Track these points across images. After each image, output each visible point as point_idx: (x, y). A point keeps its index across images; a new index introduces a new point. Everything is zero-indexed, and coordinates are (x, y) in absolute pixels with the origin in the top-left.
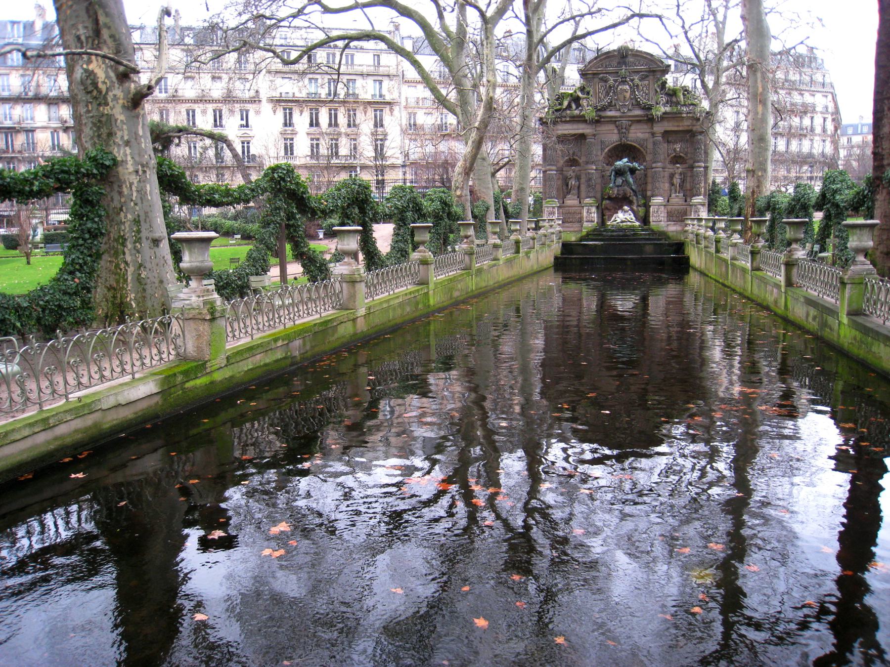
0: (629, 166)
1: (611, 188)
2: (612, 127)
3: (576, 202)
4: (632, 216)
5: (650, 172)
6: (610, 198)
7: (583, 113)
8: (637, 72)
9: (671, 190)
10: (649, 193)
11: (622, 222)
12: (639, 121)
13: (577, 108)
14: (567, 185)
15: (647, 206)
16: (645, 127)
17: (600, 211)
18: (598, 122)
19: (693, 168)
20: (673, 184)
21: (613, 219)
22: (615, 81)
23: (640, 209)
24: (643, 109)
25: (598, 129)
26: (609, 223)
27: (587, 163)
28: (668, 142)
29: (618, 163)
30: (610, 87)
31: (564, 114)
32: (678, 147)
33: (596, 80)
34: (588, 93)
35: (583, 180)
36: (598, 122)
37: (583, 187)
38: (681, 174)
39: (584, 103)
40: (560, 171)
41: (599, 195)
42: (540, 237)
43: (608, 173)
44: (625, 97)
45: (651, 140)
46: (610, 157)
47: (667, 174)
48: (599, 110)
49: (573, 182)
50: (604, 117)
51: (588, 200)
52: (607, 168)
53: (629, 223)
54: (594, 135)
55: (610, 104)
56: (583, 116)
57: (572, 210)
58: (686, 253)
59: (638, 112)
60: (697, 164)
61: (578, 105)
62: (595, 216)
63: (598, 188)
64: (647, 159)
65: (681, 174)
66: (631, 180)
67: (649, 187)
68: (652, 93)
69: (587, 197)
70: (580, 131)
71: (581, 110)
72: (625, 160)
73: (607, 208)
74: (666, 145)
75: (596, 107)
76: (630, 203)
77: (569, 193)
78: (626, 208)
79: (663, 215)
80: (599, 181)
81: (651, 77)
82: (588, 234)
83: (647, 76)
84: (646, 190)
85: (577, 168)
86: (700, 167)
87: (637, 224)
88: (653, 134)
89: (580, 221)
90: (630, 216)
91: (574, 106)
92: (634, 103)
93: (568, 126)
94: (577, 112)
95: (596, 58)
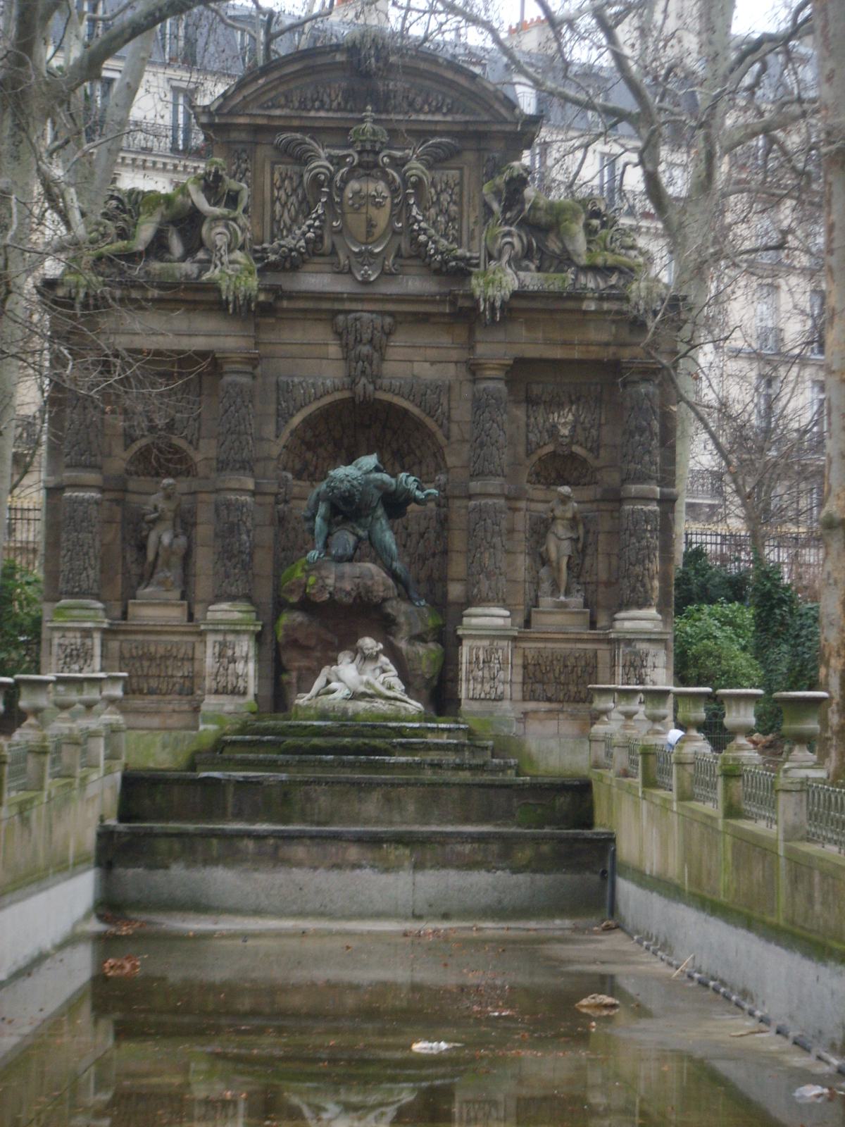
0: (381, 486)
1: (315, 567)
2: (319, 333)
3: (175, 614)
4: (392, 676)
5: (459, 511)
6: (306, 605)
7: (212, 274)
8: (421, 134)
9: (537, 582)
10: (455, 591)
11: (356, 696)
12: (422, 319)
13: (189, 253)
14: (142, 547)
15: (448, 640)
16: (445, 340)
17: (269, 653)
18: (266, 310)
19: (620, 501)
20: (544, 561)
21: (319, 683)
22: (338, 162)
23: (421, 649)
24: (437, 272)
25: (265, 337)
26: (303, 700)
27: (223, 465)
28: (531, 401)
29: (342, 471)
30: (316, 183)
31: (137, 271)
32: (564, 420)
33: (264, 152)
34: (232, 200)
35: (204, 531)
36: (266, 310)
37: (204, 560)
38: (574, 522)
39: (217, 235)
40: (116, 488)
41: (265, 592)
42: (21, 759)
43: (302, 508)
44: (370, 225)
45: (467, 391)
46: (309, 446)
47: (521, 522)
48: (273, 267)
49: (164, 536)
50: (291, 296)
51: (224, 611)
52: (298, 486)
53: (381, 706)
54: (254, 361)
55: (314, 251)
56: (213, 287)
57: (158, 645)
58: (600, 816)
59: (415, 284)
60: (634, 489)
61: (194, 244)
62: (248, 671)
63: (264, 563)
64: (451, 460)
65: (574, 522)
66: (389, 538)
67: (458, 566)
68: (472, 216)
69: (218, 599)
70: (200, 343)
71: (205, 265)
72: (370, 461)
73: (294, 644)
74: (520, 413)
75: (259, 256)
76: (384, 626)
77: (145, 578)
78: (368, 643)
79: (509, 680)
80: (266, 535)
81: (469, 157)
82: (220, 745)
83: (454, 153)
84: (444, 579)
85: (183, 485)
86: (646, 499)
87: (414, 706)
88: (474, 369)
89: (190, 688)
90: (384, 677)
91: (177, 246)
92: (405, 245)
93: (154, 321)
94: (189, 267)
95: (265, 71)
